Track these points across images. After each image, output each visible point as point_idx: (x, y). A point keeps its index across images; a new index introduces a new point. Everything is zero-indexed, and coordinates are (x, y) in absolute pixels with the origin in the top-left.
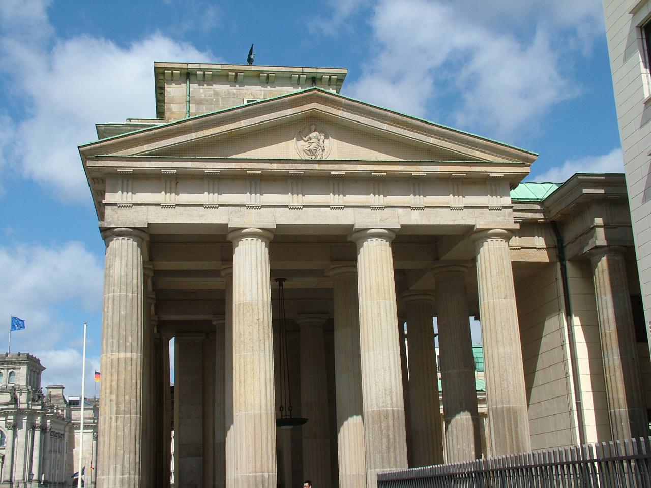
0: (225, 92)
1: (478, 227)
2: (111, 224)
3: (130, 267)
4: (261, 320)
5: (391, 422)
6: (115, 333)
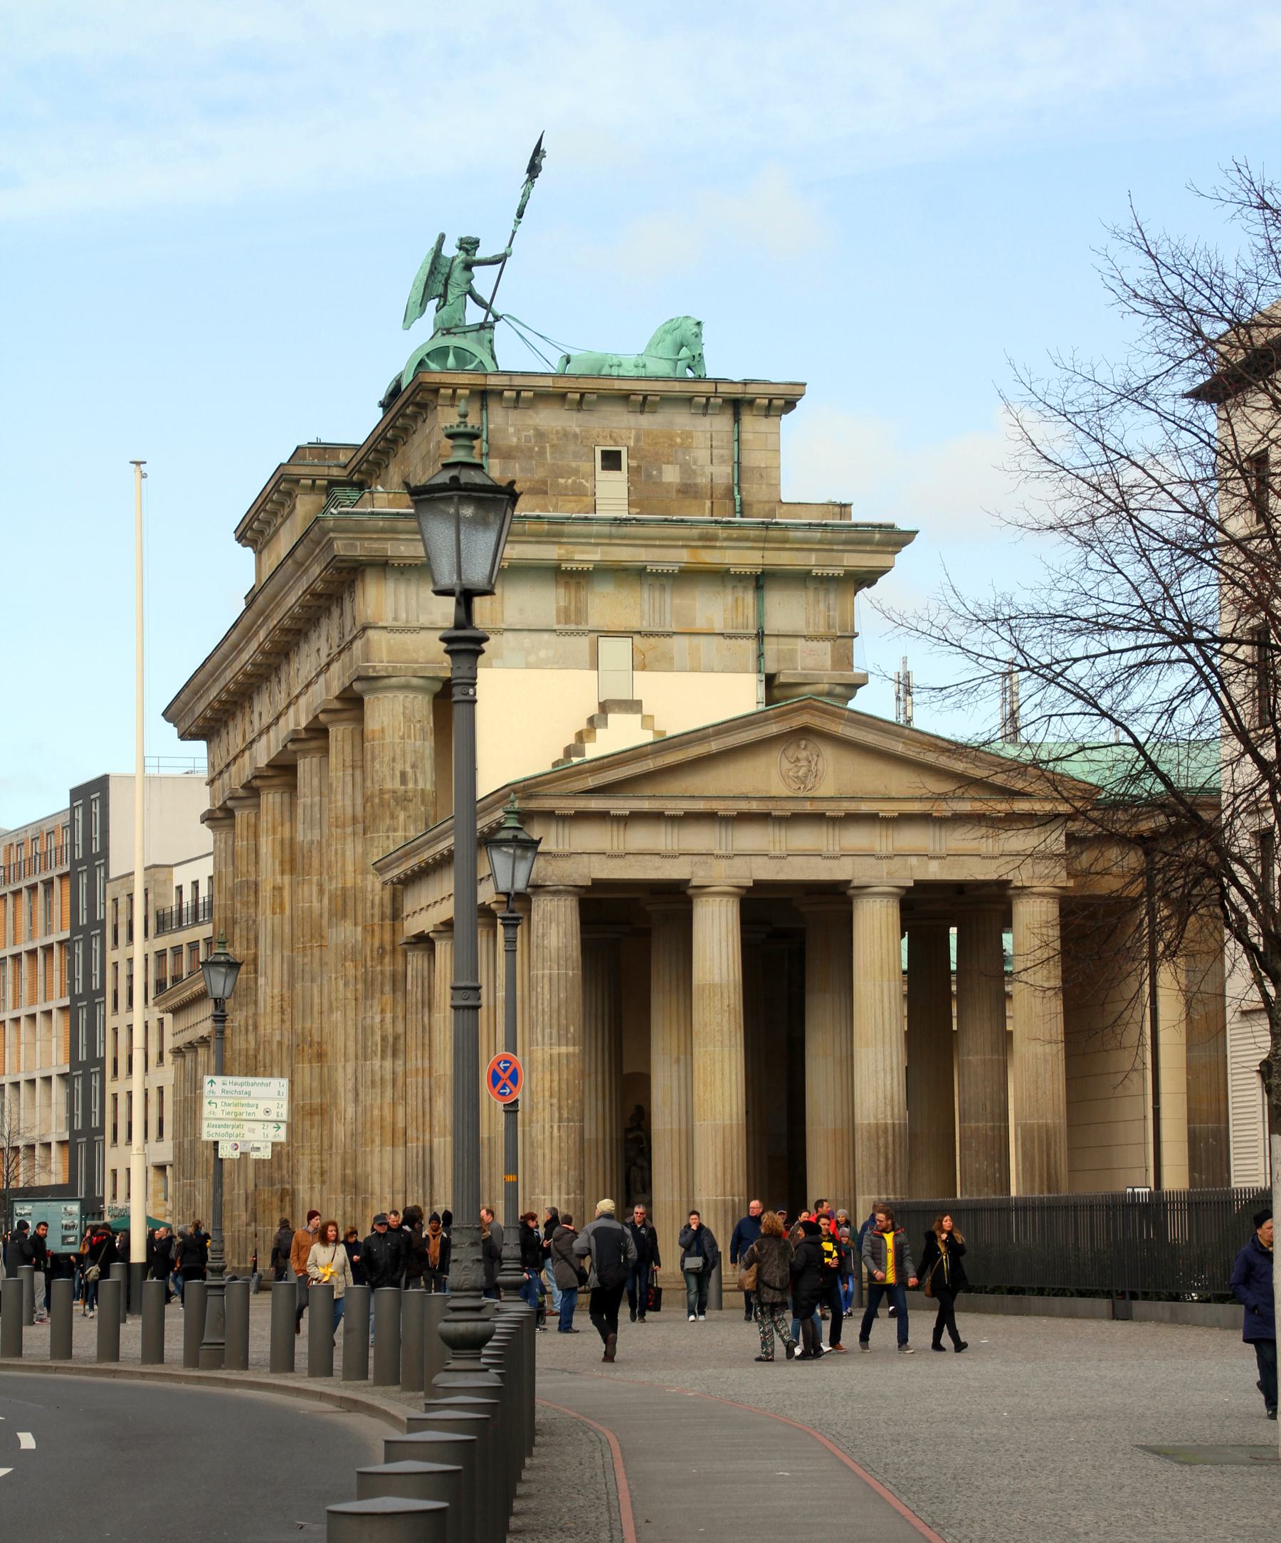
0: (557, 432)
4: (732, 1006)
6: (555, 1022)
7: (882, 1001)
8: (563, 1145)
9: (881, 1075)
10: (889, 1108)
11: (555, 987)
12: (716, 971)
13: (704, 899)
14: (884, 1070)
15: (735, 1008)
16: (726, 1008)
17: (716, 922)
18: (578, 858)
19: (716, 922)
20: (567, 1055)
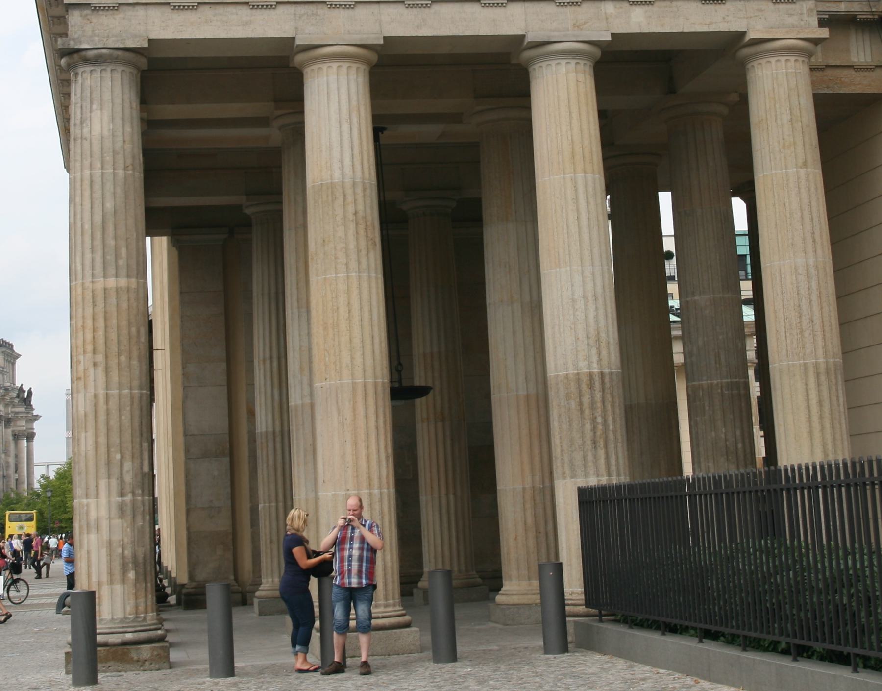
1: (751, 35)
2: (81, 42)
3: (119, 122)
4: (361, 214)
5: (598, 395)
6: (98, 242)
7: (576, 200)
8: (112, 423)
9: (580, 304)
10: (594, 351)
11: (98, 194)
12: (336, 165)
13: (315, 67)
14: (585, 297)
15: (365, 217)
16: (351, 216)
17: (334, 97)
18: (129, 12)
19: (334, 97)
20: (118, 290)
